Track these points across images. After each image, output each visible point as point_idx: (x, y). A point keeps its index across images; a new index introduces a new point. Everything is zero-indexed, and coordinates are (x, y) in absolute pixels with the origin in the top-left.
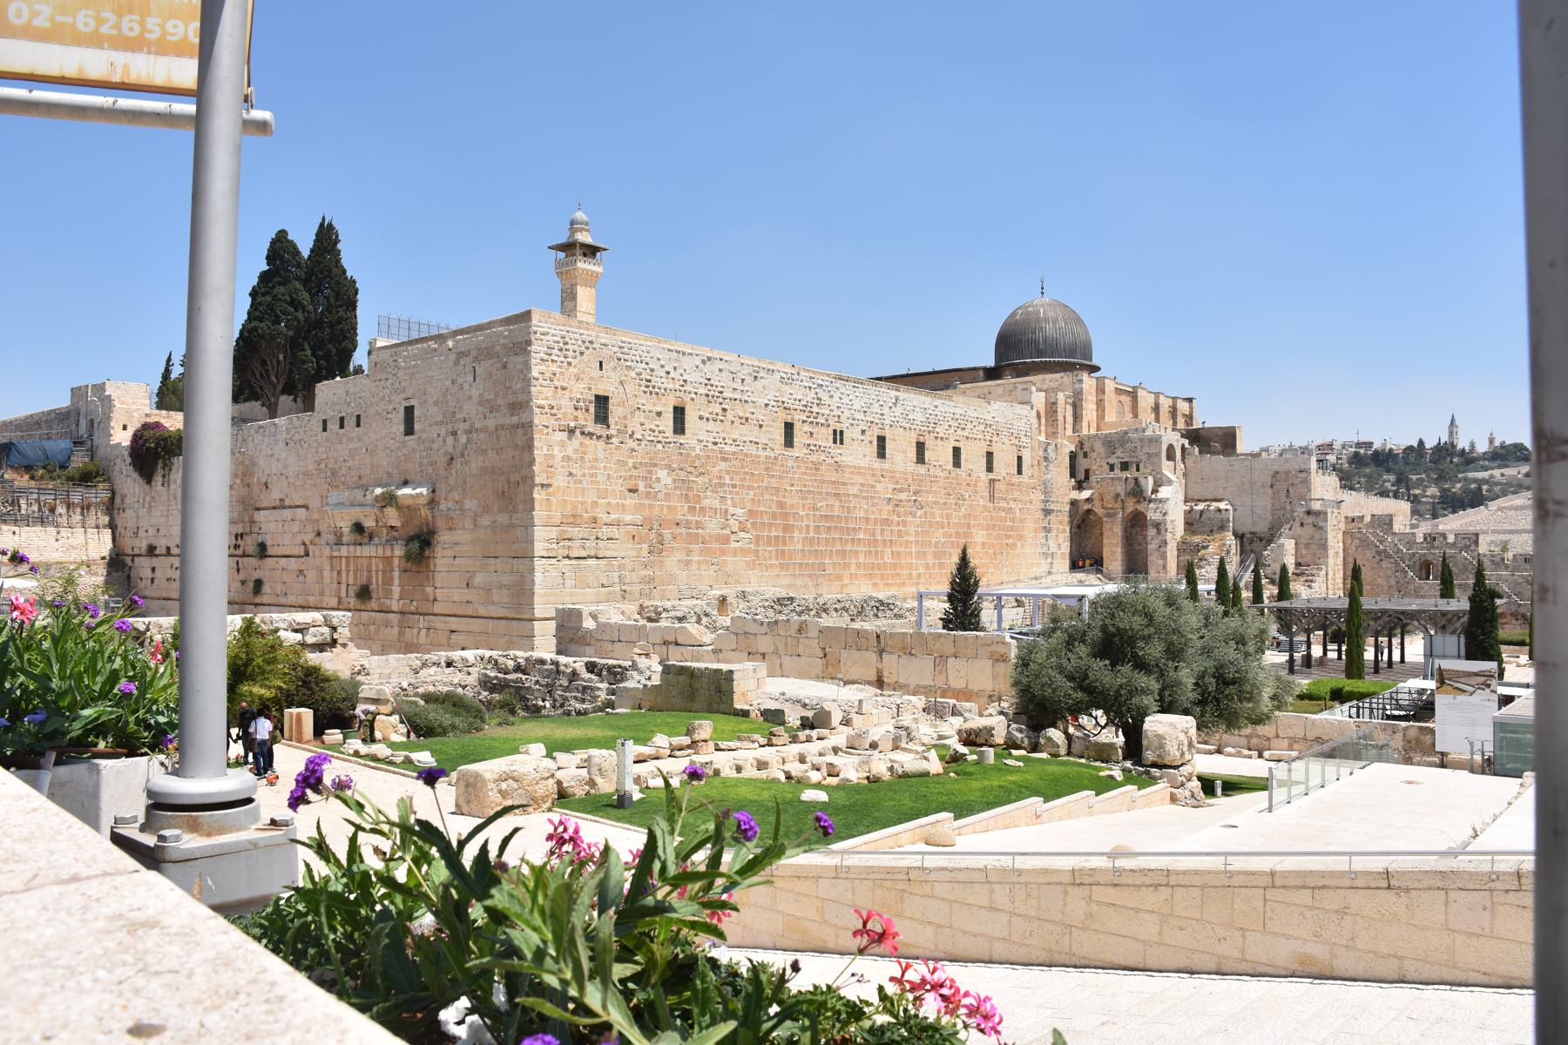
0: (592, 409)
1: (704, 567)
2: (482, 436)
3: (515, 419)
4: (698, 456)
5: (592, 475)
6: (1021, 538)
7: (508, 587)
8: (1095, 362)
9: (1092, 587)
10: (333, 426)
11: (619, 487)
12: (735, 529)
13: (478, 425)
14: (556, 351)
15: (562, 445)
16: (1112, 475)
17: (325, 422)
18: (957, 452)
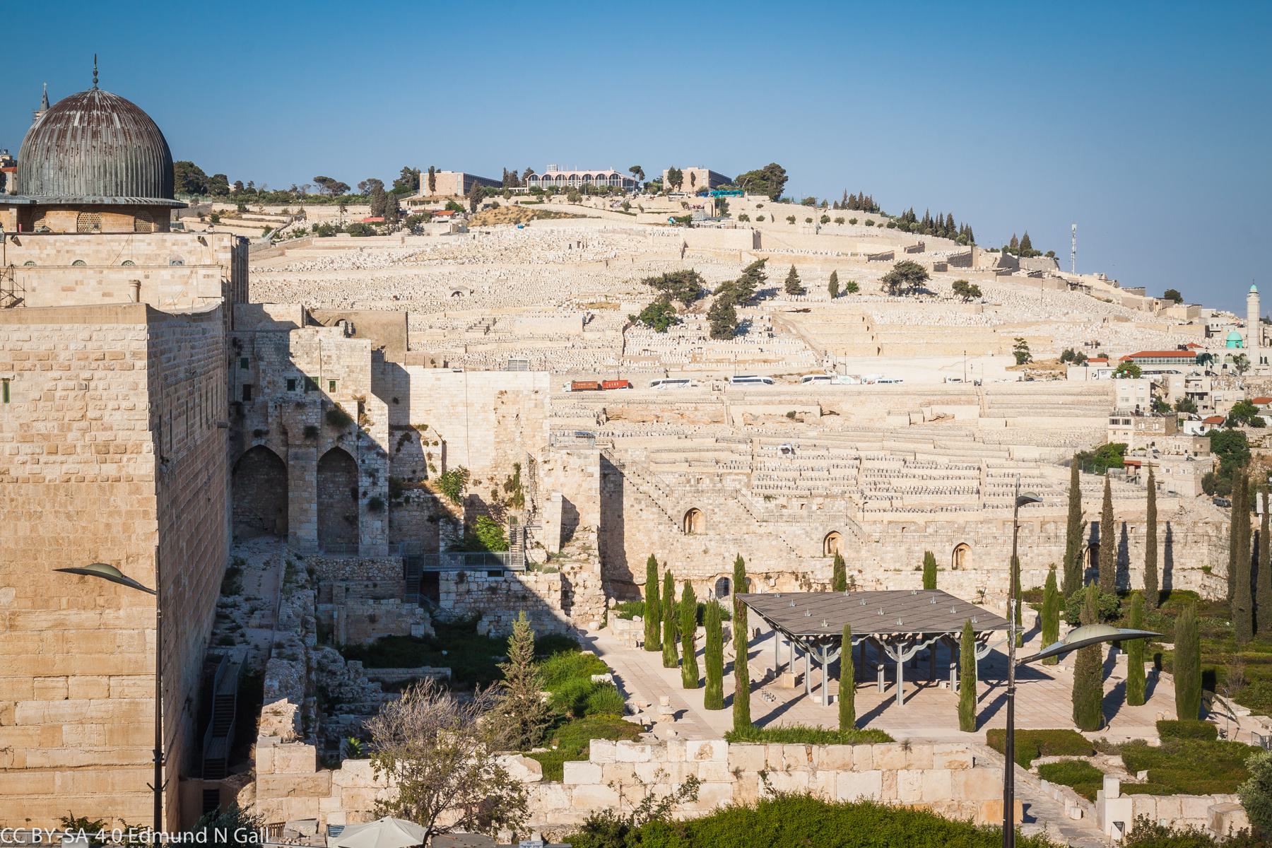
2: (31, 486)
3: (110, 469)
7: (102, 721)
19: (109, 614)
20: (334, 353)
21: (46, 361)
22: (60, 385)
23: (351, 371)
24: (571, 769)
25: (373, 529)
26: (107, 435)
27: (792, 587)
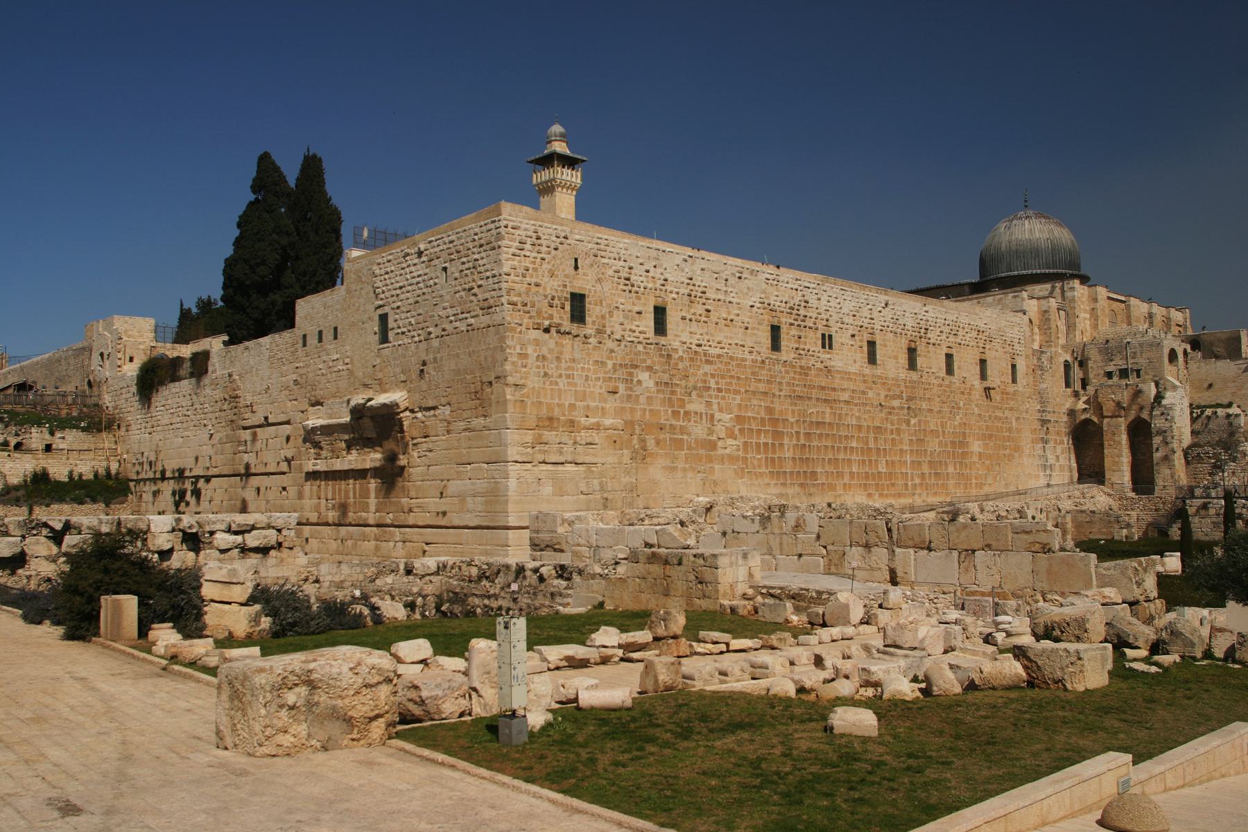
0: (568, 308)
1: (690, 475)
3: (485, 320)
4: (681, 358)
5: (568, 376)
6: (1017, 449)
8: (1083, 272)
9: (1099, 499)
10: (312, 341)
11: (599, 388)
12: (723, 435)
13: (449, 327)
14: (528, 246)
15: (537, 342)
16: (1110, 382)
17: (305, 336)
18: (949, 357)
20: (1138, 350)
22: (467, 266)
26: (487, 295)
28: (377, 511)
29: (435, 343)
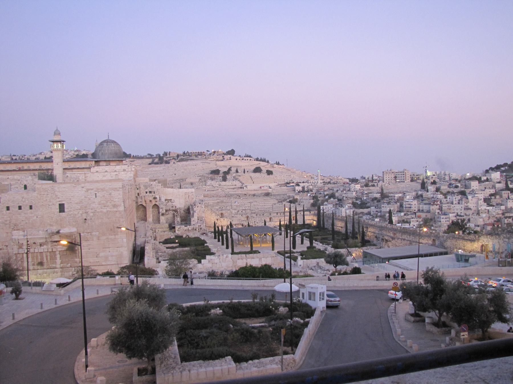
3: (115, 209)
10: (14, 209)
13: (98, 210)
19: (117, 236)
21: (103, 190)
23: (158, 189)
24: (203, 261)
25: (163, 219)
27: (241, 226)
28: (61, 263)
29: (92, 214)
